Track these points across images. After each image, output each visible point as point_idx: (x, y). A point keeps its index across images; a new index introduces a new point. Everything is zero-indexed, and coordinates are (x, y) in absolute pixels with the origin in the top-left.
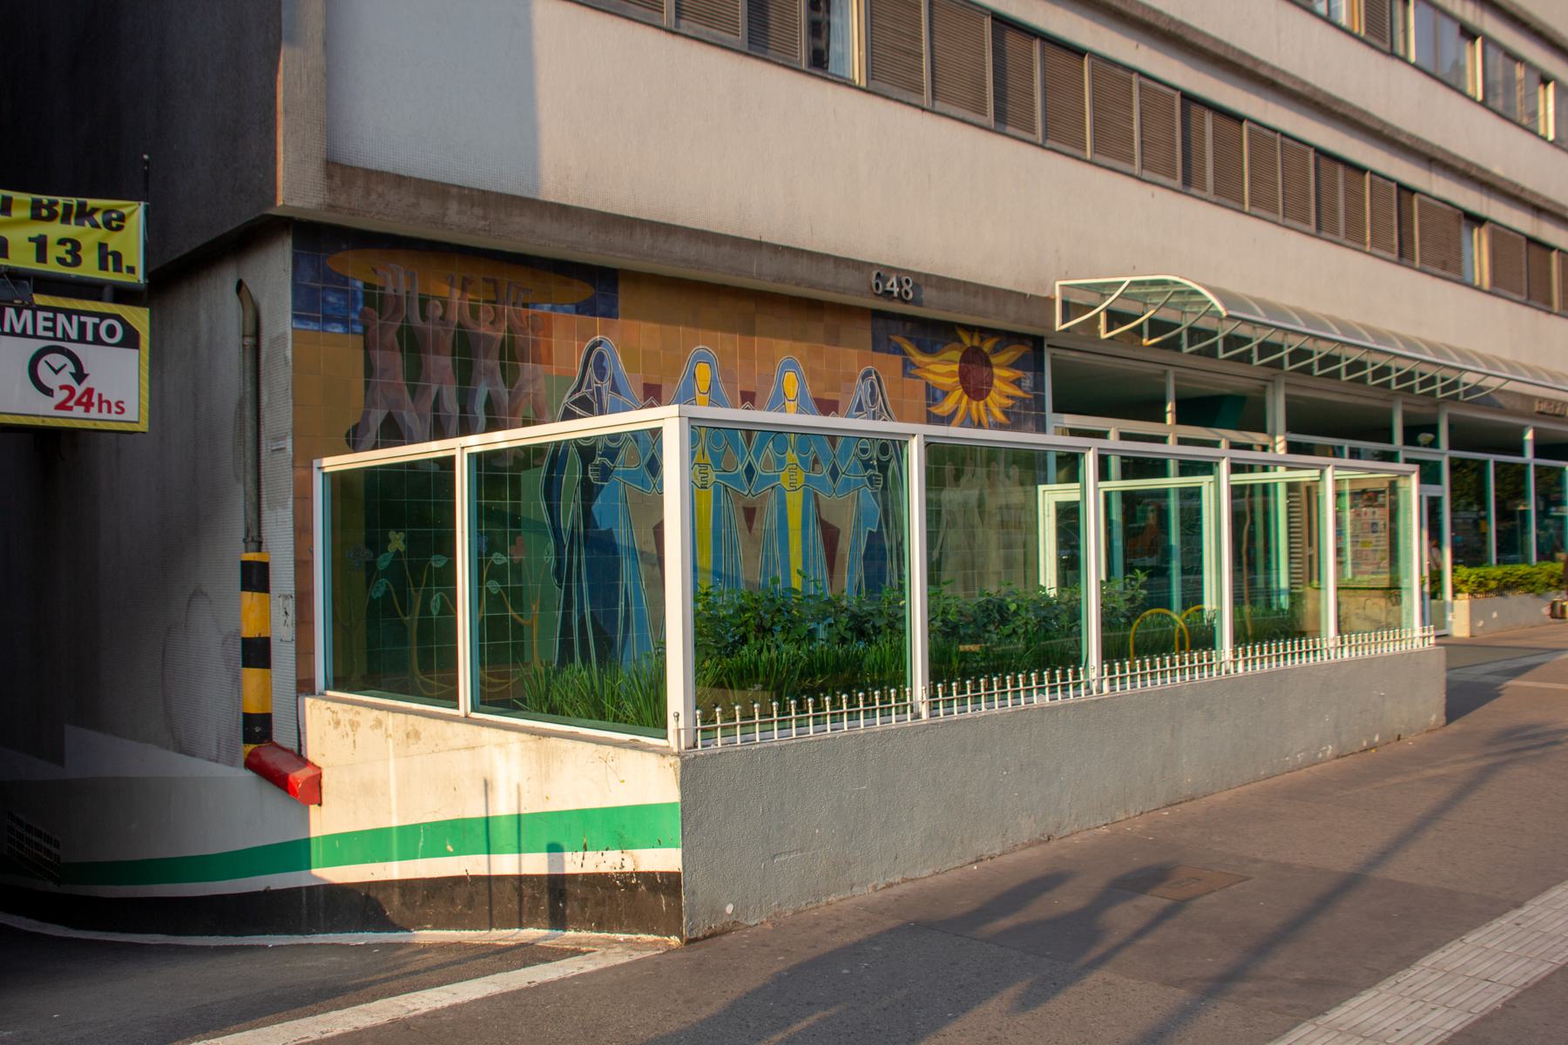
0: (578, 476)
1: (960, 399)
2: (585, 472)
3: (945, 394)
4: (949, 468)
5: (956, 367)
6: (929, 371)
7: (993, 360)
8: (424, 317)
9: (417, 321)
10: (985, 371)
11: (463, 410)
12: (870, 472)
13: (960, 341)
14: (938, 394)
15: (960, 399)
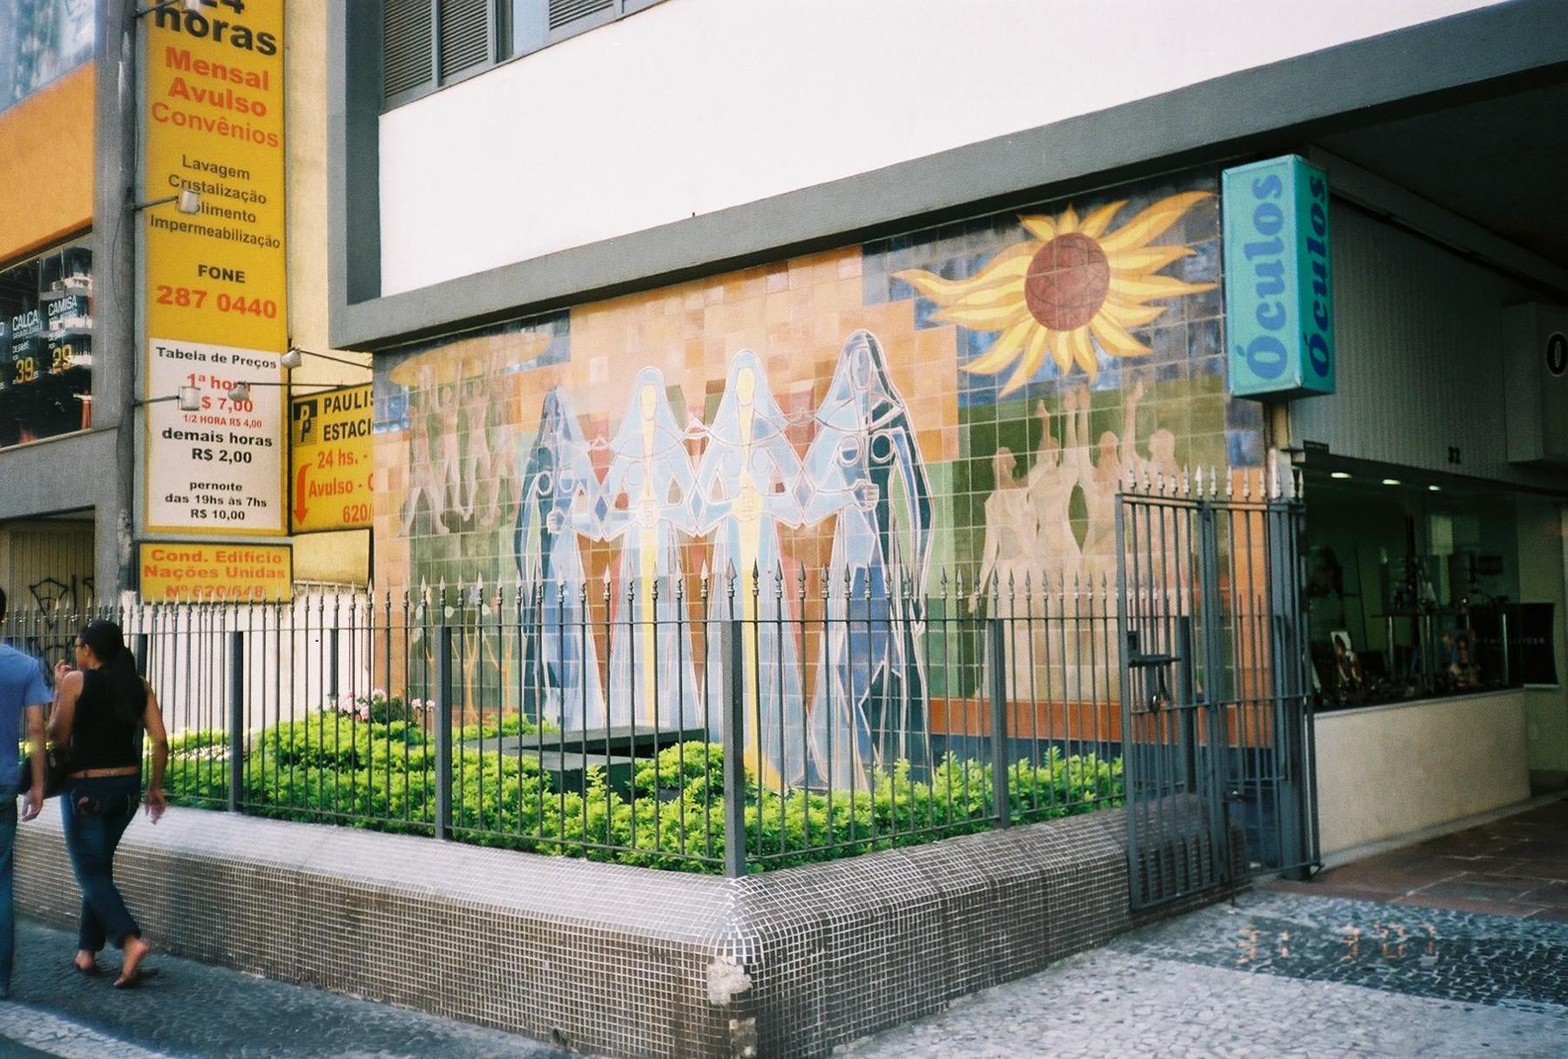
0: (539, 527)
1: (1032, 331)
2: (544, 523)
3: (994, 336)
4: (1002, 459)
5: (1020, 286)
6: (966, 307)
7: (1107, 246)
8: (441, 404)
9: (437, 410)
10: (1091, 270)
11: (462, 479)
12: (859, 482)
13: (1028, 235)
14: (981, 340)
15: (1032, 331)
